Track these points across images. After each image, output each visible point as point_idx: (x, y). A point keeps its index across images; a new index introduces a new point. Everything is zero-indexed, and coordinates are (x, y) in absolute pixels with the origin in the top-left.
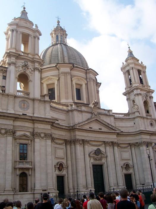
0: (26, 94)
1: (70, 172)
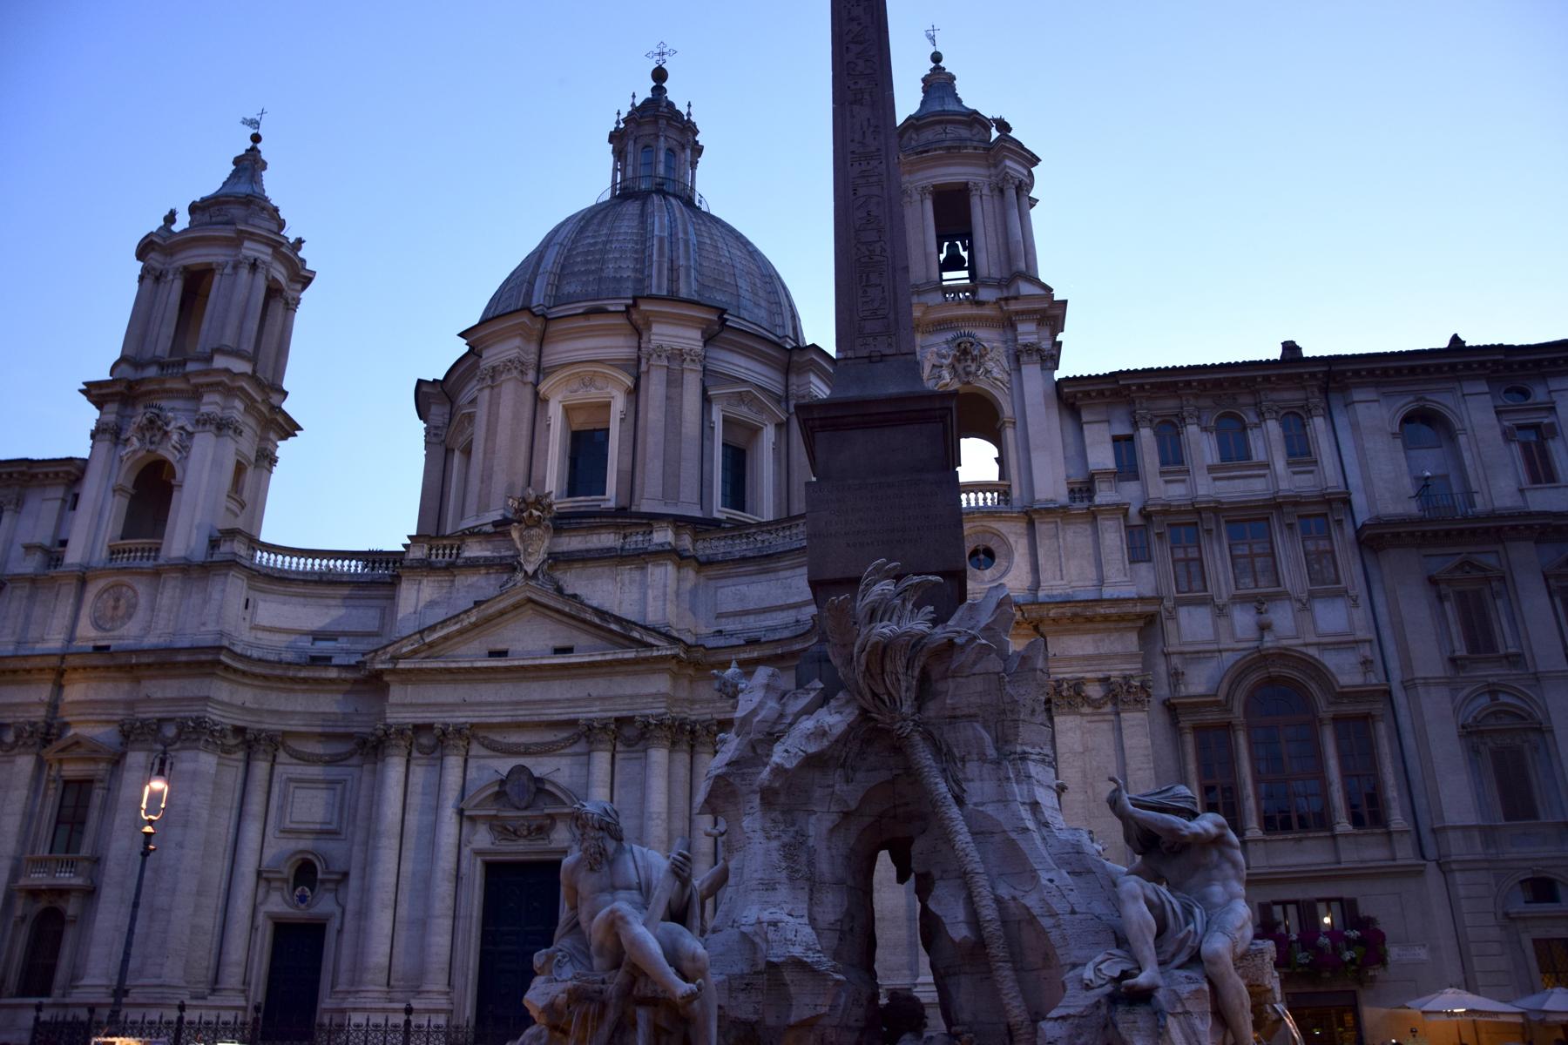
0: (143, 550)
1: (351, 907)
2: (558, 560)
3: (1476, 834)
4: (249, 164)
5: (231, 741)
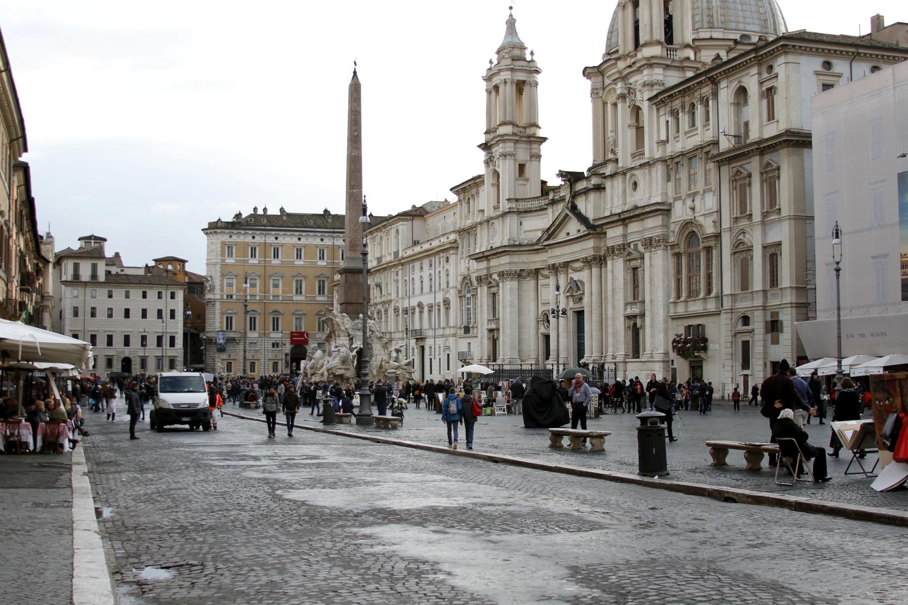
2: (575, 195)
3: (730, 297)
4: (511, 23)
5: (524, 274)
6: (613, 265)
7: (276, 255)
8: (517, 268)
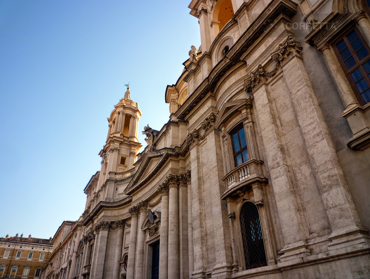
4: (127, 94)
5: (114, 226)
6: (198, 152)
7: (18, 256)
8: (109, 220)
